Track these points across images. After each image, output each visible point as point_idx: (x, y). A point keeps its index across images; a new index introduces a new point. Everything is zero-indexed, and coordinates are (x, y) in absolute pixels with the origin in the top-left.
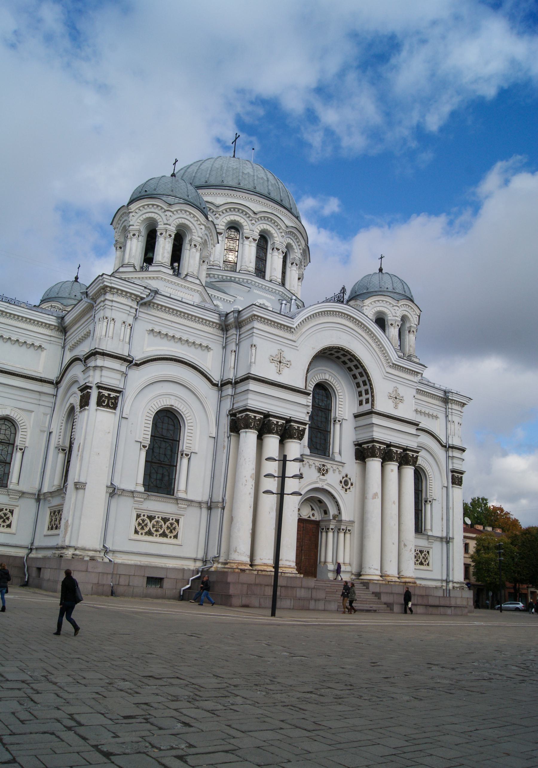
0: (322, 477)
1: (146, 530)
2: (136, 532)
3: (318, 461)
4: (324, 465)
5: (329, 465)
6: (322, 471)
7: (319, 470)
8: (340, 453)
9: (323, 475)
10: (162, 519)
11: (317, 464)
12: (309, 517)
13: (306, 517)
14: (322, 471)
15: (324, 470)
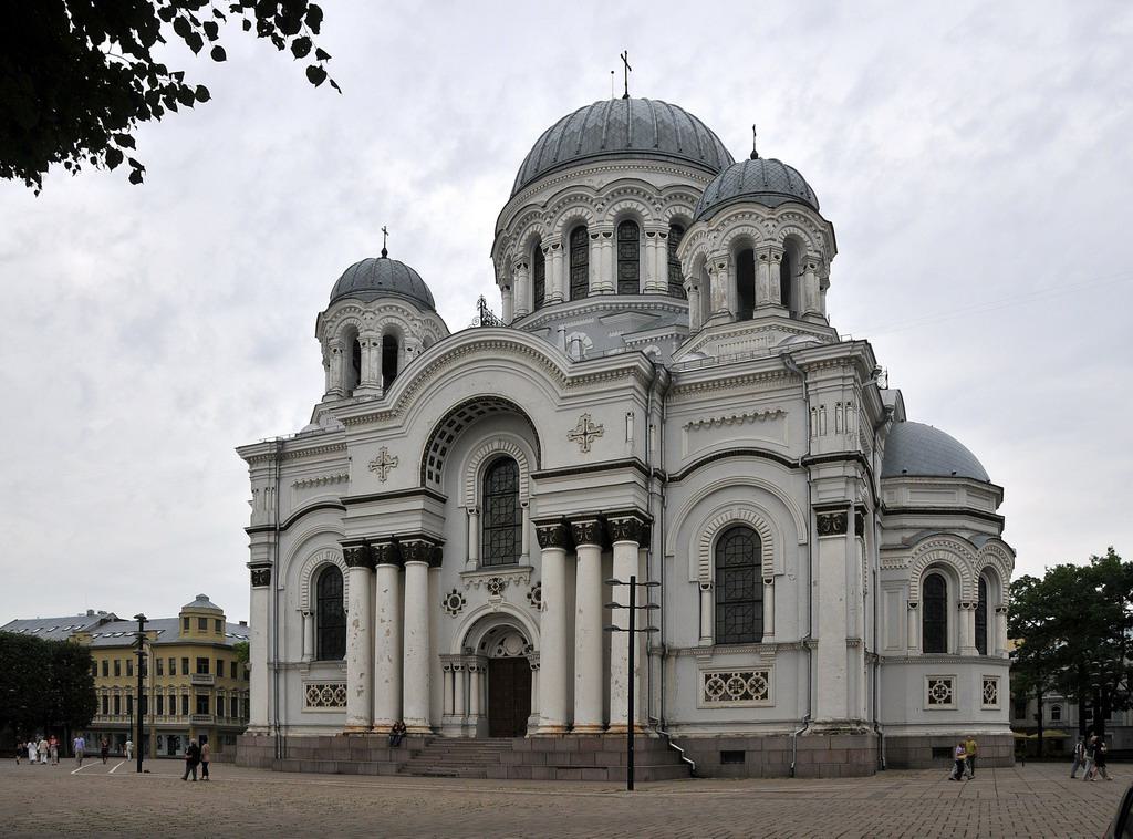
0: (497, 597)
1: (742, 692)
2: (309, 704)
3: (487, 577)
4: (495, 580)
5: (504, 575)
6: (497, 588)
7: (489, 587)
8: (528, 554)
9: (495, 593)
10: (721, 676)
11: (486, 580)
12: (521, 654)
13: (515, 656)
14: (497, 588)
15: (495, 586)
